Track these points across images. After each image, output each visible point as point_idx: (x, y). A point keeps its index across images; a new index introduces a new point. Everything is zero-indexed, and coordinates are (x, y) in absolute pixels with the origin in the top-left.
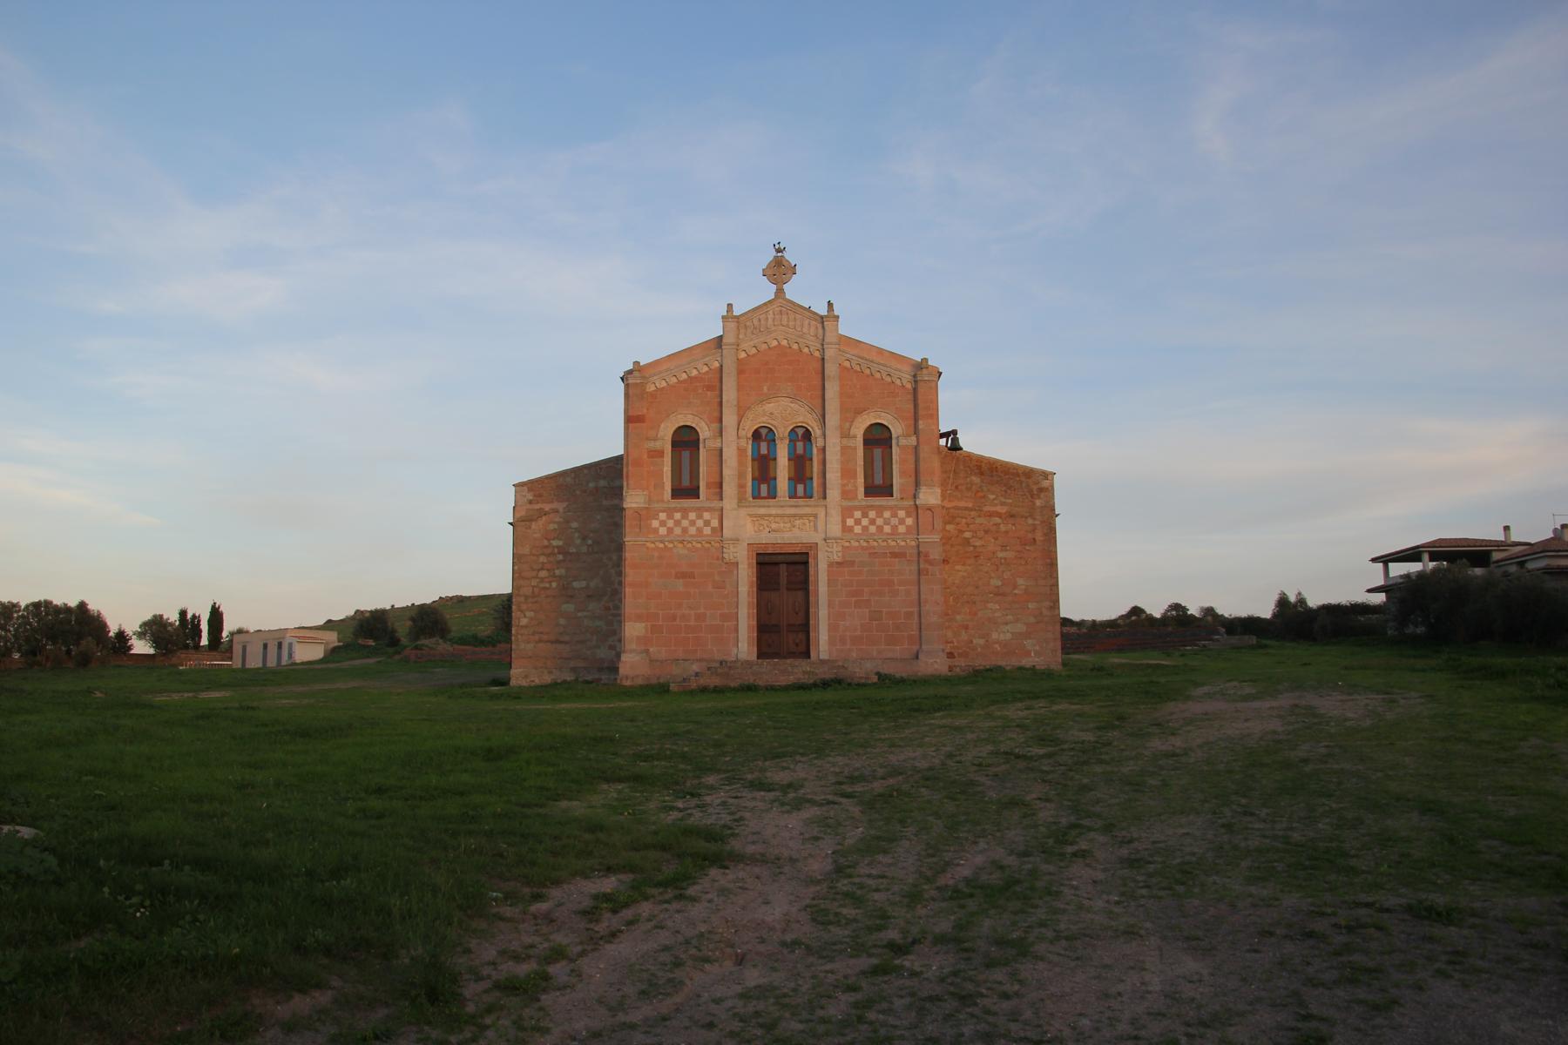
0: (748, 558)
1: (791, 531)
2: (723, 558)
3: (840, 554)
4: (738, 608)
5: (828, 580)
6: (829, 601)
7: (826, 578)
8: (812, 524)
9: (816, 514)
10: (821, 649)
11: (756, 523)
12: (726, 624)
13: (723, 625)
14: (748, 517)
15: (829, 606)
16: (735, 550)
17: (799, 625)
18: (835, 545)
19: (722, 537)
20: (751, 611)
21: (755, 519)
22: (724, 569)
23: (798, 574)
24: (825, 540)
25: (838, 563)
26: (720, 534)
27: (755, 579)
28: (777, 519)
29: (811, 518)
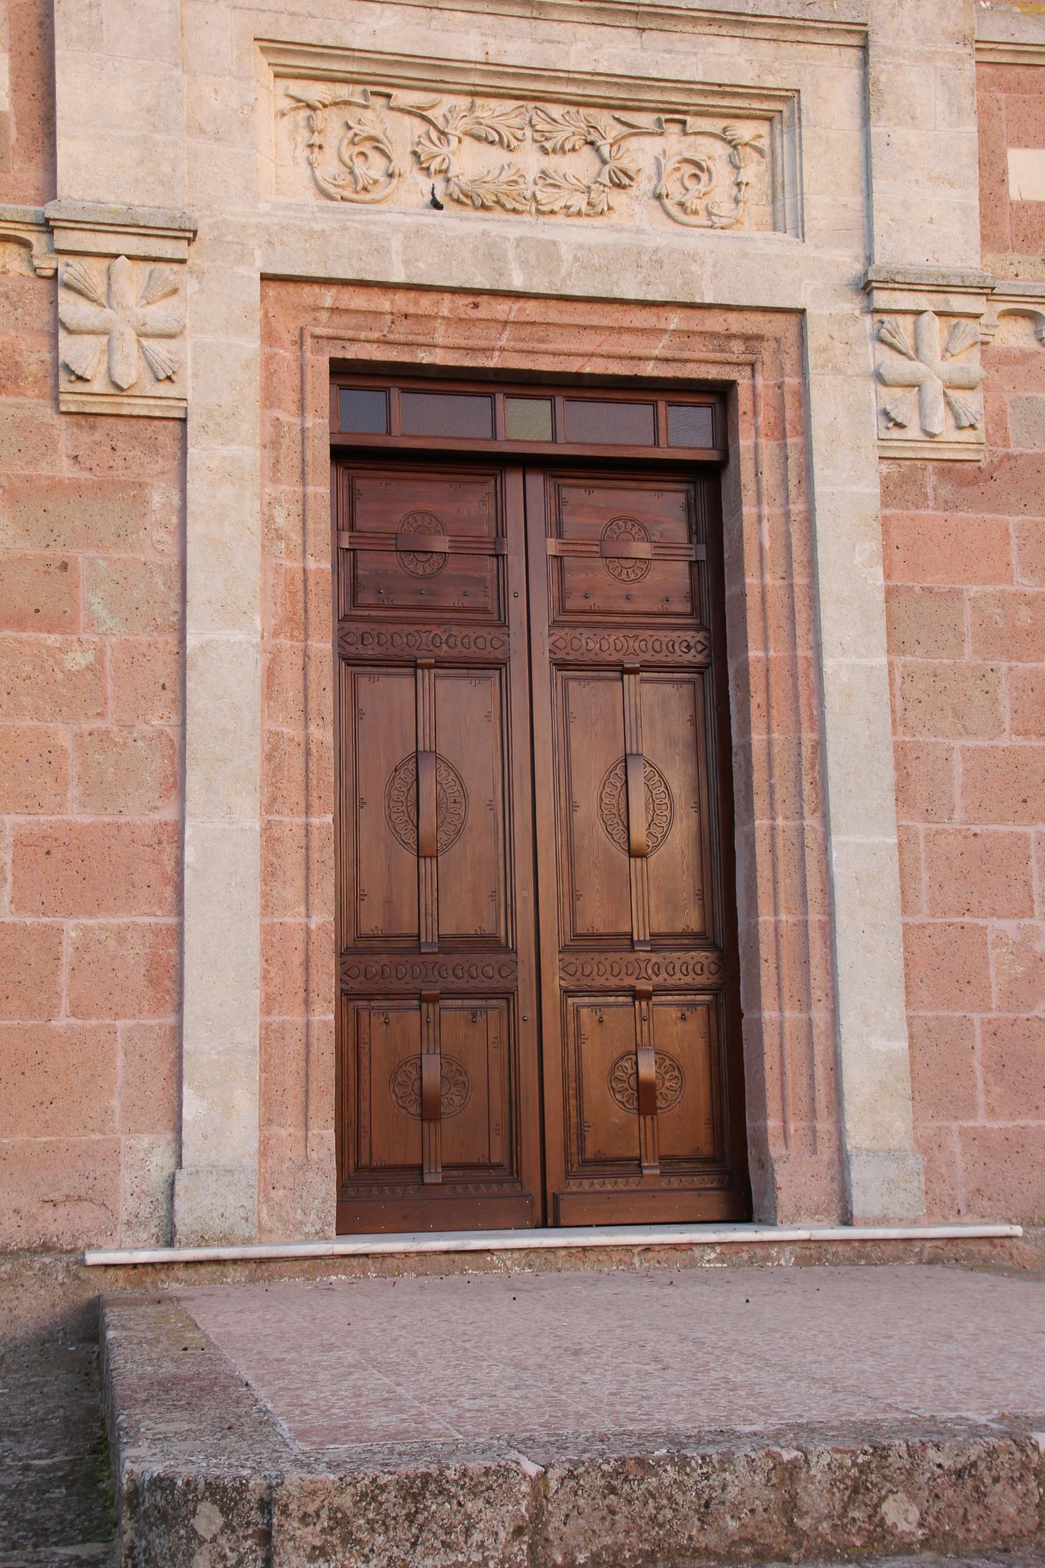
0: (269, 398)
1: (594, 211)
2: (58, 368)
3: (971, 403)
4: (178, 785)
5: (890, 593)
6: (901, 753)
7: (877, 578)
8: (753, 170)
9: (791, 96)
10: (857, 1137)
11: (332, 122)
12: (72, 928)
13: (51, 936)
14: (262, 66)
15: (902, 791)
16: (159, 315)
17: (658, 942)
18: (934, 328)
19: (50, 190)
20: (292, 821)
21: (316, 92)
22: (66, 470)
23: (642, 549)
24: (866, 288)
25: (948, 468)
26: (30, 175)
27: (321, 564)
28: (491, 110)
29: (745, 131)
